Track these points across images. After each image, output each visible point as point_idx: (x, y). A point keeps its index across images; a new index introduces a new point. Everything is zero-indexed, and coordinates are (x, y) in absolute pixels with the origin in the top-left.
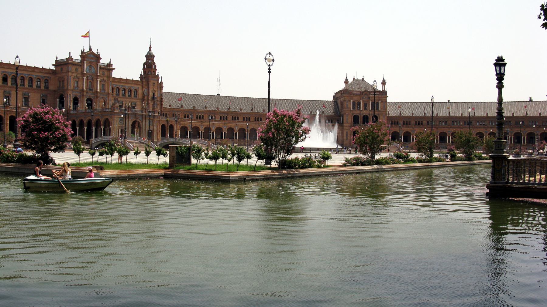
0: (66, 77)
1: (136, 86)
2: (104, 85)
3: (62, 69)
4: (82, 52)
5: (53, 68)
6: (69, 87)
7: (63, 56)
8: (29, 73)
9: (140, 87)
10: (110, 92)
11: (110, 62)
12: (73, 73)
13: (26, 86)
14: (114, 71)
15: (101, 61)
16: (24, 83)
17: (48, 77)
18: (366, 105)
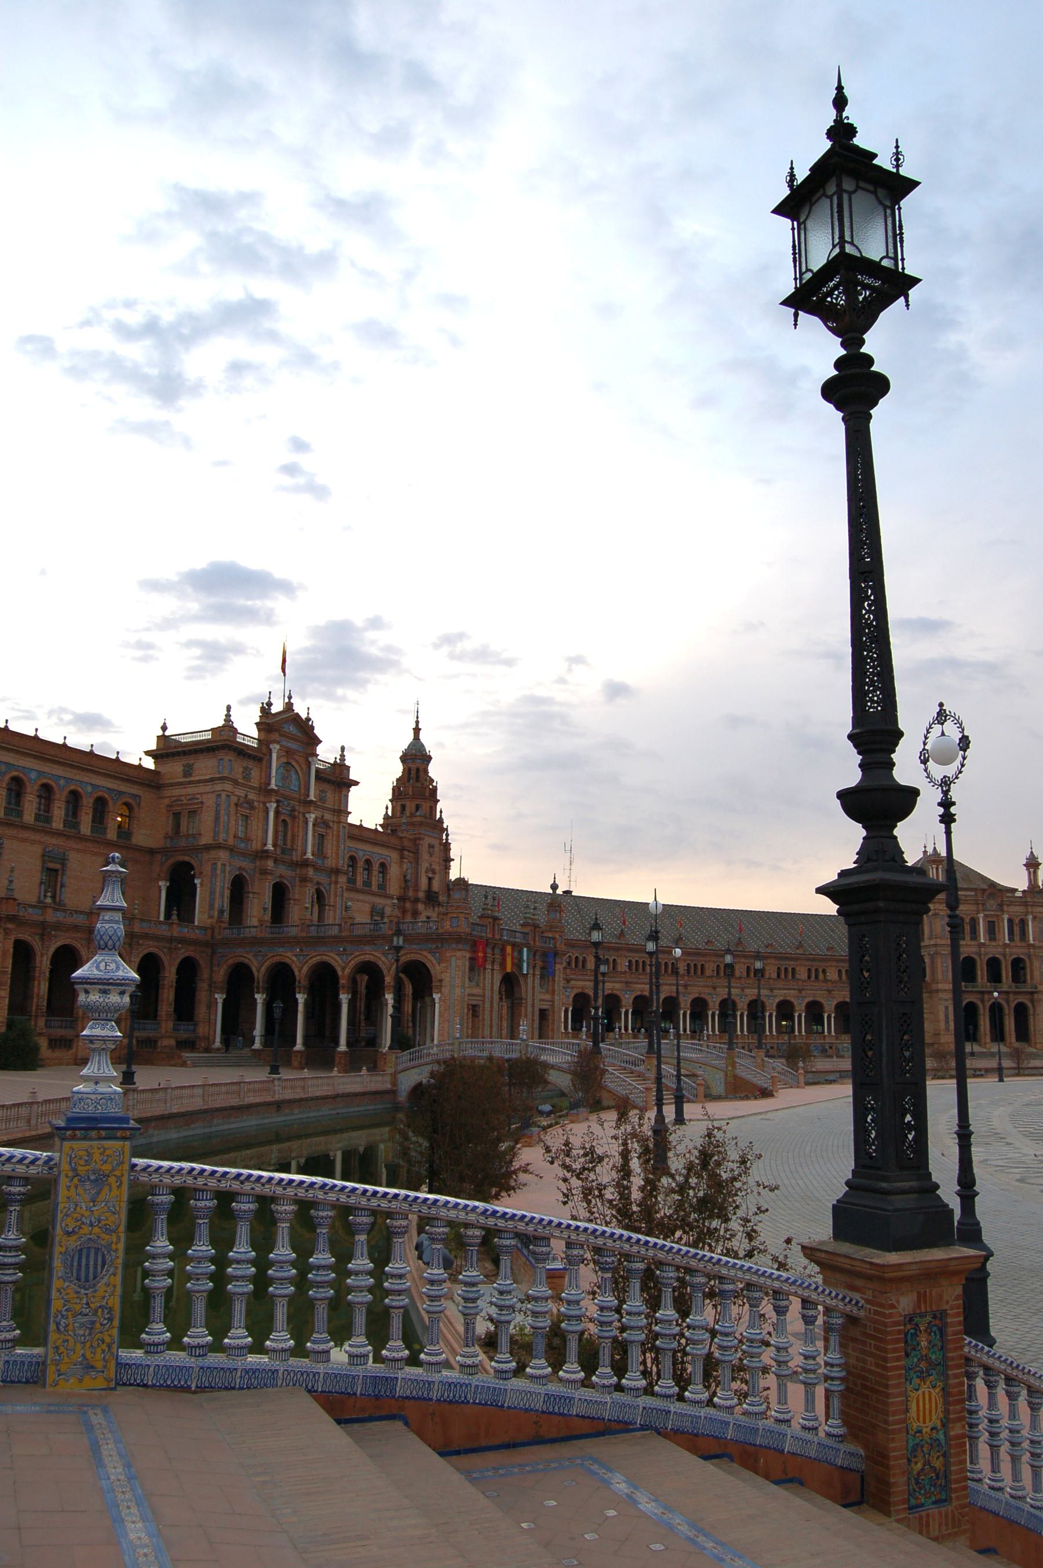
0: (210, 801)
1: (384, 852)
2: (322, 837)
3: (188, 771)
4: (265, 710)
5: (149, 763)
6: (222, 836)
7: (194, 721)
8: (69, 773)
9: (394, 855)
10: (343, 863)
11: (343, 756)
12: (236, 782)
13: (57, 824)
14: (353, 789)
15: (320, 749)
16: (48, 809)
17: (135, 796)
18: (992, 930)
